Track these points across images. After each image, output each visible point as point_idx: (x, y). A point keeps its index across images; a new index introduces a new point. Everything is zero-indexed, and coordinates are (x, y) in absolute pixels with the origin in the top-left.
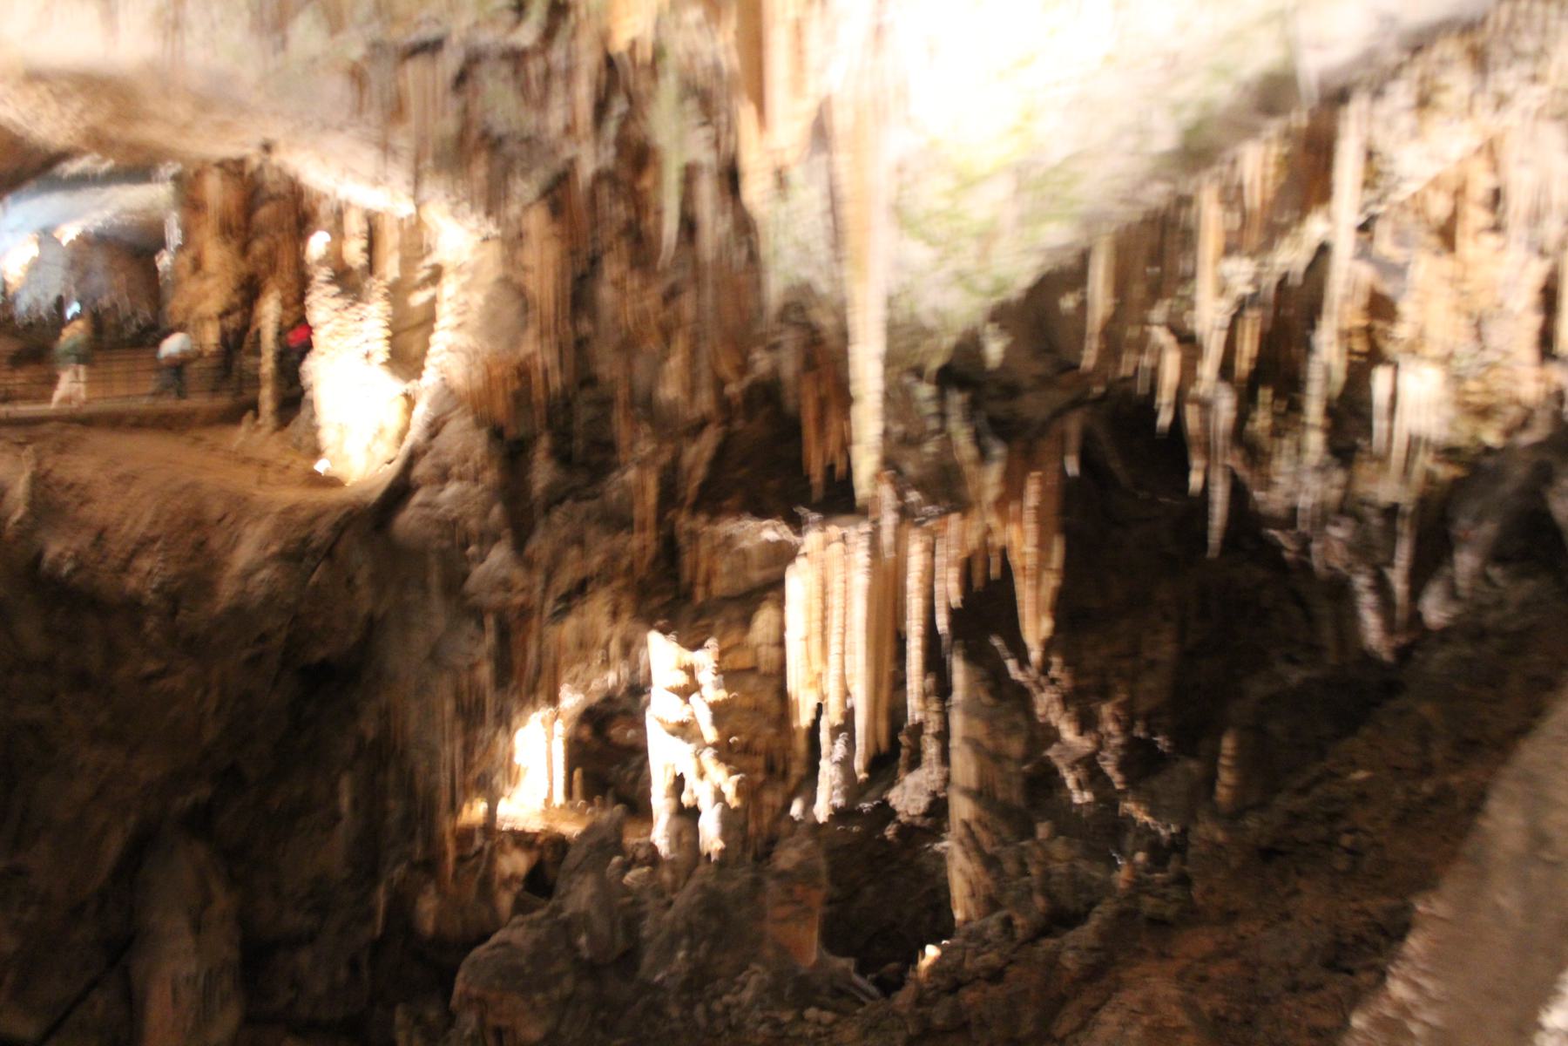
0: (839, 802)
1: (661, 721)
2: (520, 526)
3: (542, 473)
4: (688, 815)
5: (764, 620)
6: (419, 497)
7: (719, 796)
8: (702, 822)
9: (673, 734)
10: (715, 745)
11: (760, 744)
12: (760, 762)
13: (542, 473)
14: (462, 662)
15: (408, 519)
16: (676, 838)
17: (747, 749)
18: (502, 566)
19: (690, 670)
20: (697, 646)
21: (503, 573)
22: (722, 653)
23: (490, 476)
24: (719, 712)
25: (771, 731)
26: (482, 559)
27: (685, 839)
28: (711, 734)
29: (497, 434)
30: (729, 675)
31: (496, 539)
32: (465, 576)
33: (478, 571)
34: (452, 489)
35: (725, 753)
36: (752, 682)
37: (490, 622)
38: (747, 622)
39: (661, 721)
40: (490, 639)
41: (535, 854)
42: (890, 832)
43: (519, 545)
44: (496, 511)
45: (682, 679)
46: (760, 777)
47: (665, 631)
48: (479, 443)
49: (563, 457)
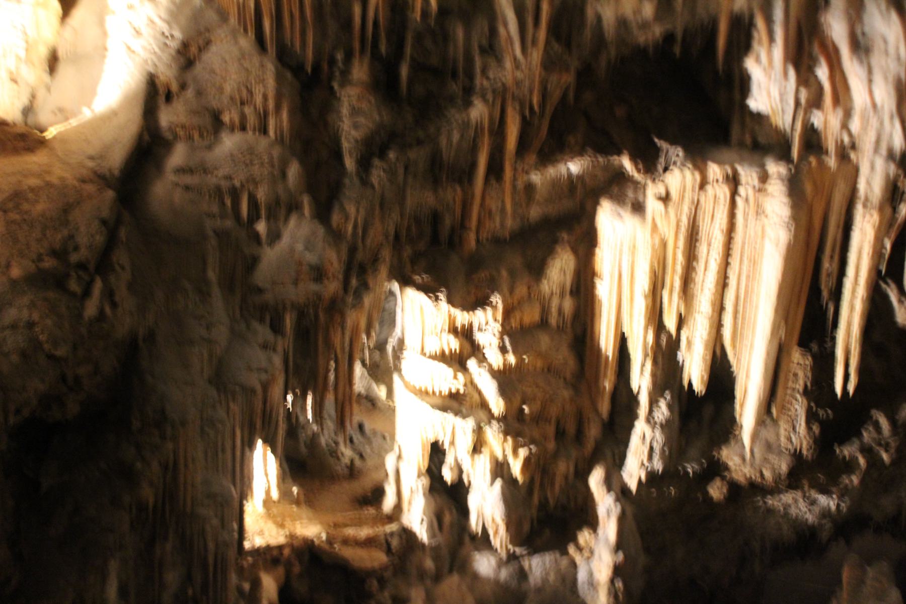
0: (658, 465)
1: (423, 394)
2: (324, 191)
3: (354, 114)
4: (449, 496)
5: (560, 268)
6: (178, 156)
7: (500, 469)
8: (474, 502)
9: (444, 409)
10: (503, 419)
11: (554, 411)
12: (551, 430)
13: (354, 114)
14: (254, 381)
15: (165, 190)
16: (437, 520)
17: (538, 418)
18: (338, 252)
19: (466, 334)
20: (481, 302)
21: (311, 258)
22: (508, 313)
23: (281, 121)
24: (505, 379)
25: (566, 394)
26: (275, 236)
27: (447, 519)
28: (497, 405)
29: (286, 59)
30: (515, 334)
31: (293, 207)
32: (253, 263)
33: (270, 256)
34: (229, 142)
35: (514, 425)
36: (545, 341)
37: (289, 321)
38: (537, 270)
39: (423, 394)
40: (286, 343)
41: (281, 570)
42: (716, 491)
43: (323, 214)
44: (294, 170)
45: (453, 344)
46: (551, 445)
47: (429, 290)
48: (266, 79)
49: (385, 85)
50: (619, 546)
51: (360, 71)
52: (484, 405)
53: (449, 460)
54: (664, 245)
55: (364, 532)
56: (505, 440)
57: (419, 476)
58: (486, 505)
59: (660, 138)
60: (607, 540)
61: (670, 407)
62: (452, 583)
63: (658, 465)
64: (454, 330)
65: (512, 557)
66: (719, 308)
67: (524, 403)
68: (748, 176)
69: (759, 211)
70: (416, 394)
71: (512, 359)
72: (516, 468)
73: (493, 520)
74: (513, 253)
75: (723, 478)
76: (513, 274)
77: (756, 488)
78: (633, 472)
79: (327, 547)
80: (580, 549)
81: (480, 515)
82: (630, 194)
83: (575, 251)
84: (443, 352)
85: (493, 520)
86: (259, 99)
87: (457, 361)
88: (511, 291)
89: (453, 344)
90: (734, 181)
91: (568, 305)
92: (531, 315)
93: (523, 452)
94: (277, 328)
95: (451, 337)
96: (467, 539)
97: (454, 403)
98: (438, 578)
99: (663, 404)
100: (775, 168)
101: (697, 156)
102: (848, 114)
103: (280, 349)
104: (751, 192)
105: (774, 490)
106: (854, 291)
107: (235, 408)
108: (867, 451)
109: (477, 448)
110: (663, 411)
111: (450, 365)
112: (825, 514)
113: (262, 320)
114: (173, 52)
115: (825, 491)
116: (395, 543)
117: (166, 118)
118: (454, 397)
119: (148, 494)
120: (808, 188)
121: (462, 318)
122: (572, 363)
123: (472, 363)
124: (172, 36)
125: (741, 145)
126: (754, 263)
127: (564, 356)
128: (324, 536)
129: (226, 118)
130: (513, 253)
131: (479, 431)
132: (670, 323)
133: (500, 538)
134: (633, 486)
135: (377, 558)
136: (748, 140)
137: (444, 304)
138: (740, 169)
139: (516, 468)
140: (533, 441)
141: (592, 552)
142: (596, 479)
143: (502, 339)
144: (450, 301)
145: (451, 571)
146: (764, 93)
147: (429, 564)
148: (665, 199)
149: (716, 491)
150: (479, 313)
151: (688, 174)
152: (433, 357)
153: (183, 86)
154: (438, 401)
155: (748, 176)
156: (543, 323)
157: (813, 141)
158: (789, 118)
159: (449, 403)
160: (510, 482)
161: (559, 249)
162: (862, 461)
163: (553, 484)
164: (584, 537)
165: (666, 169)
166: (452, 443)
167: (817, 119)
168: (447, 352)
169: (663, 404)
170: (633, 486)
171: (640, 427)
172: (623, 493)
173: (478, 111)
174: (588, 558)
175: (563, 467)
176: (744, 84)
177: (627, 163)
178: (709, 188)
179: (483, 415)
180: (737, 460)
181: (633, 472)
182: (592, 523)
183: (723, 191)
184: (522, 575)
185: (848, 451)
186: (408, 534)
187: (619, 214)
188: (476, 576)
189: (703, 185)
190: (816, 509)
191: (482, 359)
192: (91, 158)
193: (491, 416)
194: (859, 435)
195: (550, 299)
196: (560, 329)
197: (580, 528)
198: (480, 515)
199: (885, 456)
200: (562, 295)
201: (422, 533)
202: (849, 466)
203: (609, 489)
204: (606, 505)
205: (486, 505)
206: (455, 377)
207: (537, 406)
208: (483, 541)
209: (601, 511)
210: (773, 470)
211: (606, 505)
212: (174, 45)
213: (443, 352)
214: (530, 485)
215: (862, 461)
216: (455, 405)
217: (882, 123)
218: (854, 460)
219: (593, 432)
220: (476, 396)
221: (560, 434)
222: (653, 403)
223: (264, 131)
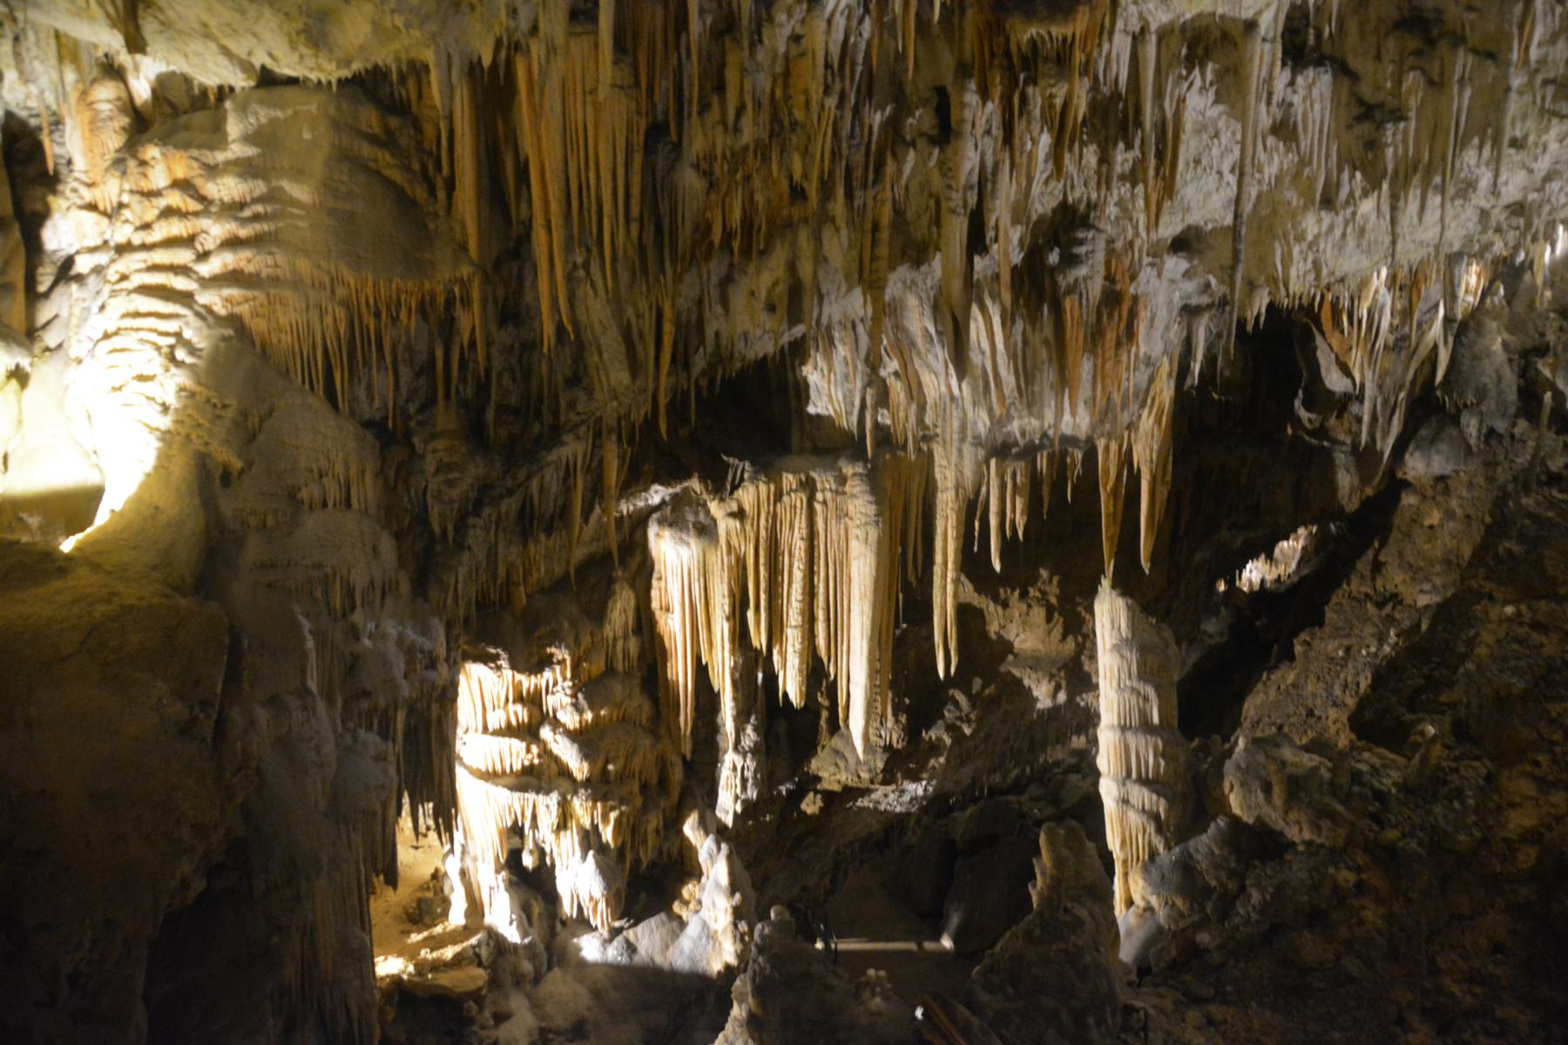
0: (752, 793)
1: (491, 776)
4: (533, 884)
6: (253, 550)
7: (590, 839)
8: (564, 885)
9: (521, 788)
11: (637, 763)
17: (622, 777)
19: (533, 701)
20: (545, 662)
22: (576, 668)
23: (367, 491)
25: (647, 741)
28: (578, 767)
30: (587, 688)
35: (600, 787)
36: (617, 688)
38: (598, 614)
39: (491, 776)
40: (394, 750)
42: (811, 805)
45: (520, 713)
49: (475, 433)
50: (734, 887)
51: (446, 418)
52: (565, 772)
53: (530, 844)
54: (741, 563)
55: (449, 953)
56: (594, 807)
57: (497, 872)
58: (580, 881)
59: (729, 455)
60: (717, 885)
61: (755, 729)
62: (557, 984)
63: (752, 793)
64: (519, 699)
65: (615, 933)
66: (810, 619)
67: (607, 762)
68: (824, 481)
69: (842, 514)
70: (487, 780)
71: (589, 716)
72: (607, 834)
73: (591, 898)
74: (571, 600)
75: (816, 792)
76: (573, 623)
77: (850, 793)
78: (727, 806)
79: (416, 979)
80: (686, 903)
81: (575, 896)
82: (691, 518)
83: (633, 586)
84: (509, 724)
85: (591, 898)
86: (339, 468)
87: (527, 732)
88: (577, 642)
89: (520, 713)
90: (809, 487)
91: (633, 645)
92: (597, 666)
93: (613, 815)
94: (386, 734)
95: (519, 707)
96: (559, 927)
97: (530, 779)
98: (537, 979)
99: (749, 729)
100: (848, 470)
101: (767, 468)
102: (922, 408)
103: (391, 758)
104: (829, 495)
105: (865, 792)
106: (944, 576)
107: (357, 839)
108: (952, 728)
109: (562, 825)
110: (750, 737)
111: (522, 739)
112: (914, 799)
113: (369, 728)
114: (227, 422)
115: (916, 778)
116: (484, 953)
117: (227, 506)
118: (528, 771)
119: (290, 970)
120: (888, 484)
121: (528, 682)
122: (647, 708)
123: (546, 733)
124: (225, 406)
125: (801, 452)
126: (842, 564)
127: (639, 705)
128: (411, 968)
129: (304, 494)
130: (571, 600)
131: (564, 806)
132: (759, 639)
133: (600, 916)
134: (729, 820)
135: (477, 976)
136: (808, 445)
137: (508, 673)
138: (813, 474)
139: (607, 834)
140: (622, 801)
141: (700, 902)
142: (690, 828)
143: (574, 696)
144: (513, 667)
145: (550, 968)
146: (825, 398)
147: (527, 966)
148: (740, 514)
149: (811, 805)
150: (547, 674)
151: (763, 488)
152: (499, 733)
153: (249, 464)
154: (511, 780)
155: (824, 481)
156: (610, 670)
157: (884, 437)
158: (854, 419)
159: (525, 779)
160: (602, 849)
161: (617, 587)
162: (948, 741)
163: (645, 842)
164: (687, 890)
165: (735, 488)
166: (534, 825)
167: (885, 418)
168: (514, 722)
169: (749, 729)
170: (729, 820)
171: (730, 758)
172: (721, 833)
173: (572, 449)
174: (697, 912)
175: (654, 821)
176: (802, 391)
177: (695, 484)
178: (785, 498)
179: (565, 784)
180: (833, 769)
181: (727, 806)
182: (695, 873)
183: (799, 499)
184: (631, 948)
185: (933, 734)
186: (494, 938)
187: (682, 540)
188: (583, 964)
189: (779, 496)
190: (906, 798)
191: (556, 724)
192: (154, 568)
193: (575, 785)
194: (943, 717)
195: (614, 646)
196: (628, 673)
197: (683, 883)
198: (575, 896)
199: (967, 731)
200: (626, 637)
201: (513, 935)
202: (935, 748)
203: (707, 834)
204: (704, 846)
205: (580, 881)
206: (528, 751)
207: (621, 761)
208: (583, 923)
209: (703, 857)
210: (870, 770)
211: (704, 846)
212: (230, 414)
213: (509, 724)
214: (621, 851)
215: (948, 741)
216: (533, 781)
217: (965, 414)
218: (939, 739)
219: (677, 774)
220: (553, 766)
221: (644, 787)
222: (739, 731)
223: (349, 505)
